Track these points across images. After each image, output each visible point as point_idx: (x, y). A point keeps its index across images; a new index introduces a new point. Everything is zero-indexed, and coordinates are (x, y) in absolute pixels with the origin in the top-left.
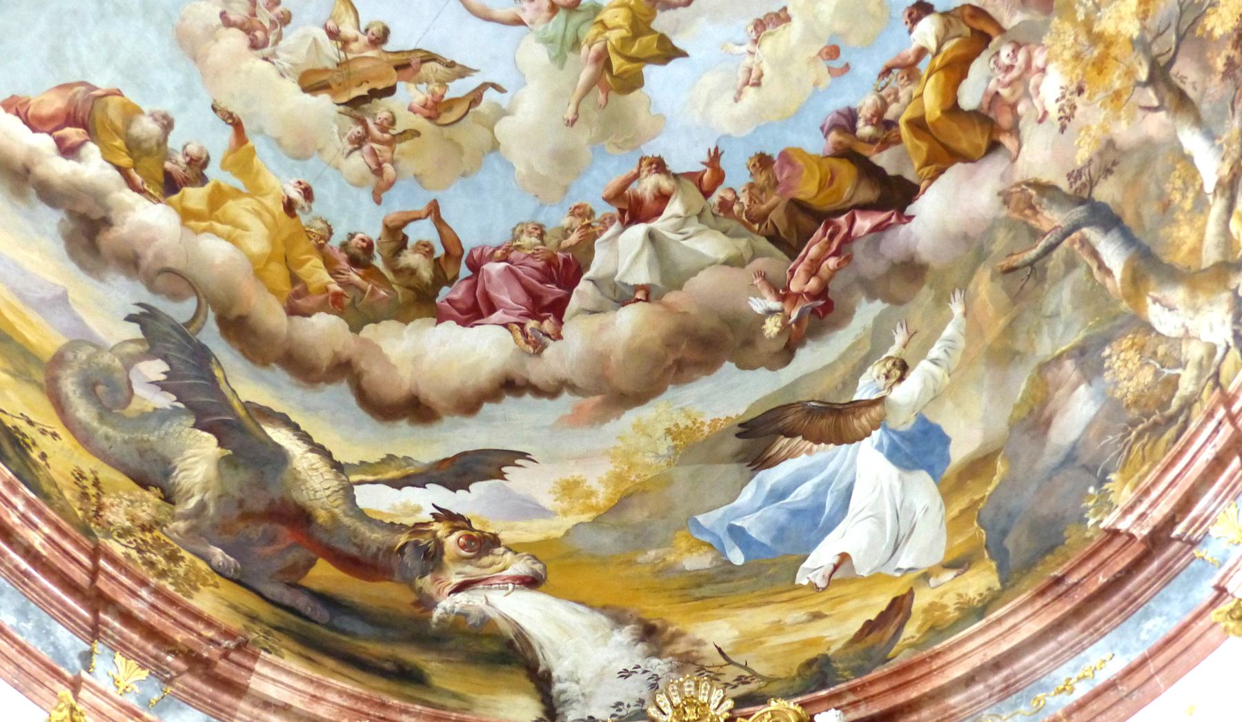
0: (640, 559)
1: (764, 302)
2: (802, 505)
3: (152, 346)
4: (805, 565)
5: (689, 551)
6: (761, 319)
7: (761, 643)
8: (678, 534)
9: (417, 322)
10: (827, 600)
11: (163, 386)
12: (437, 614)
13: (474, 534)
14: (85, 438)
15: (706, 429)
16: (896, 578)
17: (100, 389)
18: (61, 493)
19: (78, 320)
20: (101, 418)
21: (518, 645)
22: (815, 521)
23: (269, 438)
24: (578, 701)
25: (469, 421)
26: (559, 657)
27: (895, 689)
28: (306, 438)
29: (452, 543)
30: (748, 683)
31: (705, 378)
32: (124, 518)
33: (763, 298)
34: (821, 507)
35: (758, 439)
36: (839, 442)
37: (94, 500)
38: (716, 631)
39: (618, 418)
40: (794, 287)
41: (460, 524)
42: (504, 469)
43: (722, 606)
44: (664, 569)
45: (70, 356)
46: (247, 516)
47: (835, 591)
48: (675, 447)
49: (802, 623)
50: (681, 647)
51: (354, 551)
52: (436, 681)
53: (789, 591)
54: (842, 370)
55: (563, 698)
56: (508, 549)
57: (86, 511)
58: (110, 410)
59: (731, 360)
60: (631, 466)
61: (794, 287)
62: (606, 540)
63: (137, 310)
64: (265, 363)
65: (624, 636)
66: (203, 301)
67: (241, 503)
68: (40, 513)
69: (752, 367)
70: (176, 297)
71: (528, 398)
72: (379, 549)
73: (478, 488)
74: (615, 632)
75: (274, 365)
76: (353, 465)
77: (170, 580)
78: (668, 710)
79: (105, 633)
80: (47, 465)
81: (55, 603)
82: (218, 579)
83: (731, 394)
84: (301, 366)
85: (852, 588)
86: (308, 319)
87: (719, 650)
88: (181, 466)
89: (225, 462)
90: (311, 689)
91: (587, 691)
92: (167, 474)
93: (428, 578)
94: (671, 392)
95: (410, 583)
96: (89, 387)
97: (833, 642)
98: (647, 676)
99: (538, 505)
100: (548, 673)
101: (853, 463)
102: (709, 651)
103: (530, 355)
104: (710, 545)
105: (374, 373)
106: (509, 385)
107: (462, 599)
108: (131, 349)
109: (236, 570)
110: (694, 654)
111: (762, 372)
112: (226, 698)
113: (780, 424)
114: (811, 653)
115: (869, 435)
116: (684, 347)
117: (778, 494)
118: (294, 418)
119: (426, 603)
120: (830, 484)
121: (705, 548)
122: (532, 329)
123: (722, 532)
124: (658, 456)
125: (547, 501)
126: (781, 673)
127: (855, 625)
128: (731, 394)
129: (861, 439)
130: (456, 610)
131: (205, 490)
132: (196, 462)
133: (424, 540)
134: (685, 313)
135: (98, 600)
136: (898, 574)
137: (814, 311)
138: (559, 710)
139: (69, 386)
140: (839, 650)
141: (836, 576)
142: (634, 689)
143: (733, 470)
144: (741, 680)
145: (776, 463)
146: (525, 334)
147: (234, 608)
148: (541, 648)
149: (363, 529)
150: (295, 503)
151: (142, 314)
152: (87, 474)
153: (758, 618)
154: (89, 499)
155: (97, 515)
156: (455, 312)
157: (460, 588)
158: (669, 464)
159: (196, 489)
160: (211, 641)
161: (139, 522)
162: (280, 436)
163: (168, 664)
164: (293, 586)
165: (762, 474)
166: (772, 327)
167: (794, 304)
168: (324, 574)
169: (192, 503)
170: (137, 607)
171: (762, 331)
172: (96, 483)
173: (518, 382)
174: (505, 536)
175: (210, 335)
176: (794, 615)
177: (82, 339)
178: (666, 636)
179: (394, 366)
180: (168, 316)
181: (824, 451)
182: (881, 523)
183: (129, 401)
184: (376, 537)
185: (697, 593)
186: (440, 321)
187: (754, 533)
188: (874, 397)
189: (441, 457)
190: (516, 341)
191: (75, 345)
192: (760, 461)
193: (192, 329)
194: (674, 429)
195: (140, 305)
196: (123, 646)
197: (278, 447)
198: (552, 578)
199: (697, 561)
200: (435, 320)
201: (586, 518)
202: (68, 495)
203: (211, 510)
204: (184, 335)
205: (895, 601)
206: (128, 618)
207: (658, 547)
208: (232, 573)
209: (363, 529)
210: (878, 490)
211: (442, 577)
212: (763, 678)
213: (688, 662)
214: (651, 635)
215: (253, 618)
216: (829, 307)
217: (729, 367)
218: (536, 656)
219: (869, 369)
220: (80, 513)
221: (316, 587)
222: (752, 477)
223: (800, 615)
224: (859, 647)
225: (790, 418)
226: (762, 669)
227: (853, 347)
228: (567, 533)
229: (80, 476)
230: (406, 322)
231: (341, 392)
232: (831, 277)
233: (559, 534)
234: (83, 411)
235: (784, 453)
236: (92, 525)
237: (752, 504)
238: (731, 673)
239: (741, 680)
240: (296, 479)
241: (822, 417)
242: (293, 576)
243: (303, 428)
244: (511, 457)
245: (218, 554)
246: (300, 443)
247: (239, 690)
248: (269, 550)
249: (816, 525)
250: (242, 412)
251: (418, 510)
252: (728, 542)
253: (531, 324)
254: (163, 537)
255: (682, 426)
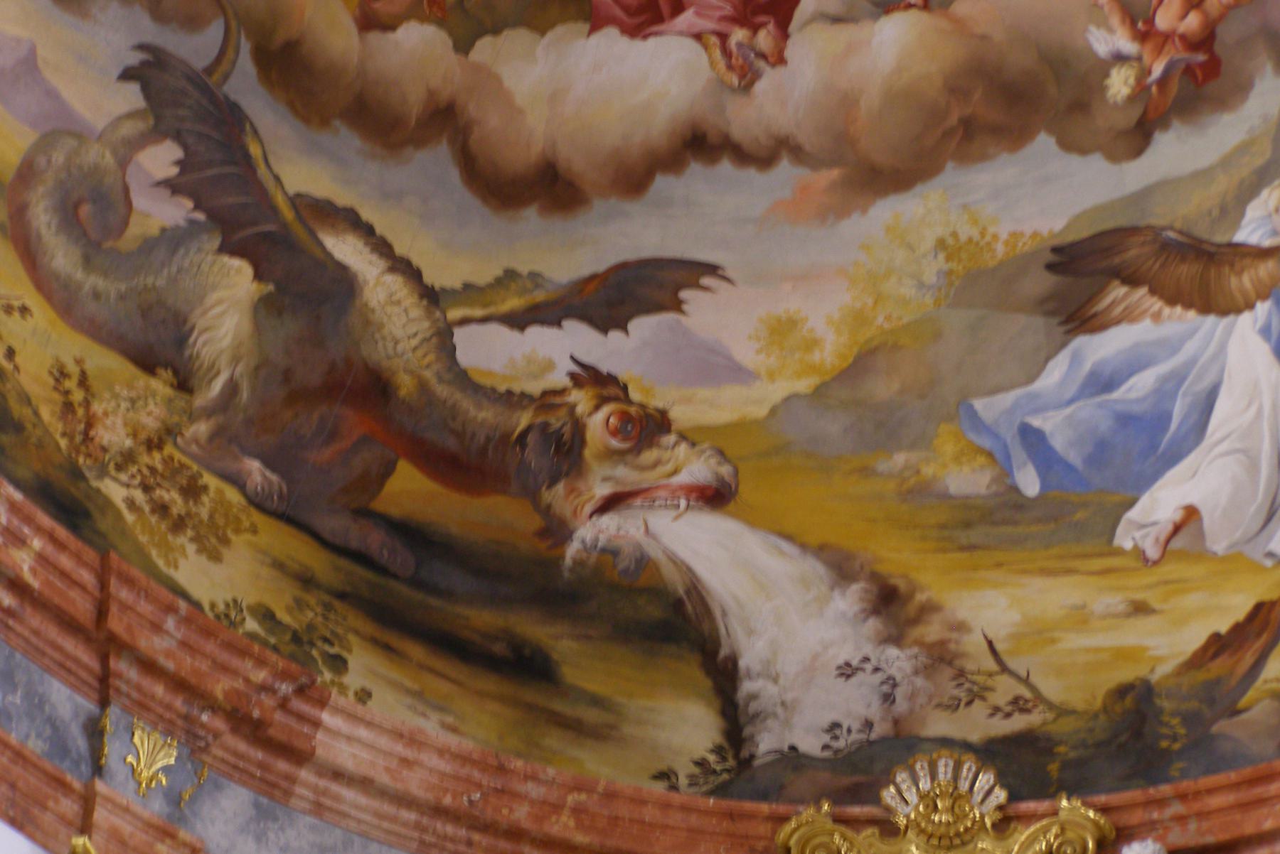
0: (883, 466)
1: (1109, 39)
2: (1137, 409)
3: (158, 119)
4: (1133, 514)
5: (957, 459)
6: (1104, 67)
7: (1053, 641)
8: (944, 428)
9: (560, 30)
10: (1158, 584)
11: (173, 187)
12: (572, 550)
13: (633, 410)
14: (63, 300)
15: (1000, 249)
16: (1264, 569)
17: (86, 210)
18: (36, 413)
19: (52, 94)
20: (87, 263)
21: (689, 608)
22: (1153, 440)
23: (329, 255)
24: (775, 715)
25: (634, 208)
26: (750, 632)
27: (1245, 806)
28: (382, 247)
29: (598, 424)
30: (1028, 711)
31: (1005, 157)
32: (122, 431)
33: (1111, 30)
34: (1168, 417)
35: (1082, 277)
36: (1206, 307)
37: (81, 412)
38: (990, 608)
39: (864, 211)
40: (1163, 20)
41: (612, 391)
42: (684, 294)
43: (999, 565)
44: (919, 492)
45: (41, 161)
46: (298, 397)
47: (1170, 570)
48: (950, 273)
49: (1116, 616)
50: (932, 631)
51: (451, 443)
52: (570, 674)
53: (1101, 555)
54: (1222, 185)
55: (753, 707)
56: (683, 437)
57: (71, 438)
58: (98, 245)
59: (1050, 131)
60: (879, 299)
61: (1163, 20)
62: (833, 426)
63: (135, 58)
64: (325, 122)
65: (848, 601)
66: (234, 24)
67: (287, 375)
68: (28, 520)
69: (1083, 151)
70: (193, 23)
71: (726, 167)
72: (488, 439)
73: (643, 326)
74: (836, 593)
75: (337, 123)
76: (453, 292)
77: (190, 533)
78: (912, 797)
79: (118, 690)
80: (17, 368)
81: (49, 650)
82: (258, 518)
83: (1042, 193)
84: (381, 123)
85: (1194, 571)
86: (391, 36)
87: (990, 643)
88: (201, 324)
89: (266, 308)
90: (399, 748)
91: (789, 697)
92: (181, 341)
93: (560, 488)
94: (951, 175)
95: (532, 495)
96: (69, 216)
97: (1160, 660)
98: (879, 677)
99: (730, 358)
100: (733, 660)
101: (1222, 349)
102: (973, 643)
103: (733, 90)
104: (990, 455)
105: (489, 121)
106: (698, 144)
107: (609, 523)
108: (130, 129)
109: (281, 496)
110: (952, 646)
111: (1097, 162)
112: (282, 765)
113: (1117, 260)
114: (1126, 674)
115: (1250, 306)
116: (977, 95)
117: (1102, 382)
118: (367, 214)
119: (557, 531)
120: (1184, 379)
121: (981, 460)
122: (740, 45)
123: (1010, 435)
124: (921, 285)
125: (746, 353)
126: (1080, 706)
127: (1194, 638)
128: (1042, 193)
129: (1239, 311)
130: (600, 544)
131: (235, 360)
132: (223, 313)
133: (556, 421)
134: (984, 37)
135: (108, 645)
136: (1269, 563)
137: (1189, 70)
138: (747, 731)
139: (42, 217)
140: (1168, 677)
141: (1177, 543)
142: (854, 704)
143: (1034, 327)
144: (1018, 705)
145: (1103, 327)
146: (727, 53)
147: (279, 566)
148: (724, 614)
149: (466, 404)
150: (366, 365)
151: (144, 64)
152: (73, 369)
153: (1053, 596)
154: (74, 412)
155: (87, 438)
156: (618, 12)
157: (610, 504)
158: (937, 303)
159: (223, 362)
160: (264, 688)
161: (143, 436)
162: (345, 249)
163: (203, 726)
164: (363, 513)
165: (1081, 341)
166: (1120, 84)
167: (1159, 51)
168: (409, 489)
169: (217, 386)
170: (157, 645)
171: (1103, 89)
172: (83, 382)
173: (713, 138)
174: (681, 415)
175: (245, 86)
176: (1107, 599)
177: (60, 129)
178: (911, 609)
179: (521, 112)
180: (183, 62)
181: (1180, 320)
182: (1253, 466)
183: (126, 223)
184: (484, 415)
185: (965, 537)
186: (594, 28)
187: (1058, 443)
188: (1267, 243)
189: (586, 271)
190: (712, 64)
191: (47, 141)
192: (1079, 318)
193: (216, 77)
194: (950, 241)
195: (142, 47)
196: (141, 706)
197: (342, 268)
198: (746, 492)
199: (968, 481)
200: (587, 27)
201: (804, 385)
202: (46, 413)
203: (245, 394)
204: (206, 90)
205: (1259, 607)
206: (149, 666)
207: (912, 446)
208: (275, 503)
209: (466, 404)
210: (1253, 410)
211: (581, 485)
212: (1051, 706)
213: (941, 659)
214: (890, 603)
215: (306, 581)
216: (1213, 68)
217: (1044, 142)
218: (716, 630)
219: (1265, 193)
220: (63, 443)
221: (395, 512)
222: (1064, 345)
223: (1115, 601)
224: (1201, 676)
225: (1132, 253)
226: (1051, 688)
227: (1243, 149)
228: (773, 411)
229: (62, 374)
230: (541, 29)
231: (437, 161)
232: (1222, 17)
233: (761, 412)
234: (62, 257)
235: (1118, 310)
236: (81, 460)
237: (1058, 394)
238: (1005, 690)
239: (1018, 705)
240: (367, 323)
241: (1183, 259)
242: (360, 495)
243: (379, 230)
244: (697, 272)
245: (254, 467)
246: (374, 258)
247: (300, 756)
248: (327, 454)
249: (1153, 447)
250: (288, 214)
251: (549, 366)
252: (1018, 453)
253: (739, 35)
254: (178, 456)
255: (963, 237)
